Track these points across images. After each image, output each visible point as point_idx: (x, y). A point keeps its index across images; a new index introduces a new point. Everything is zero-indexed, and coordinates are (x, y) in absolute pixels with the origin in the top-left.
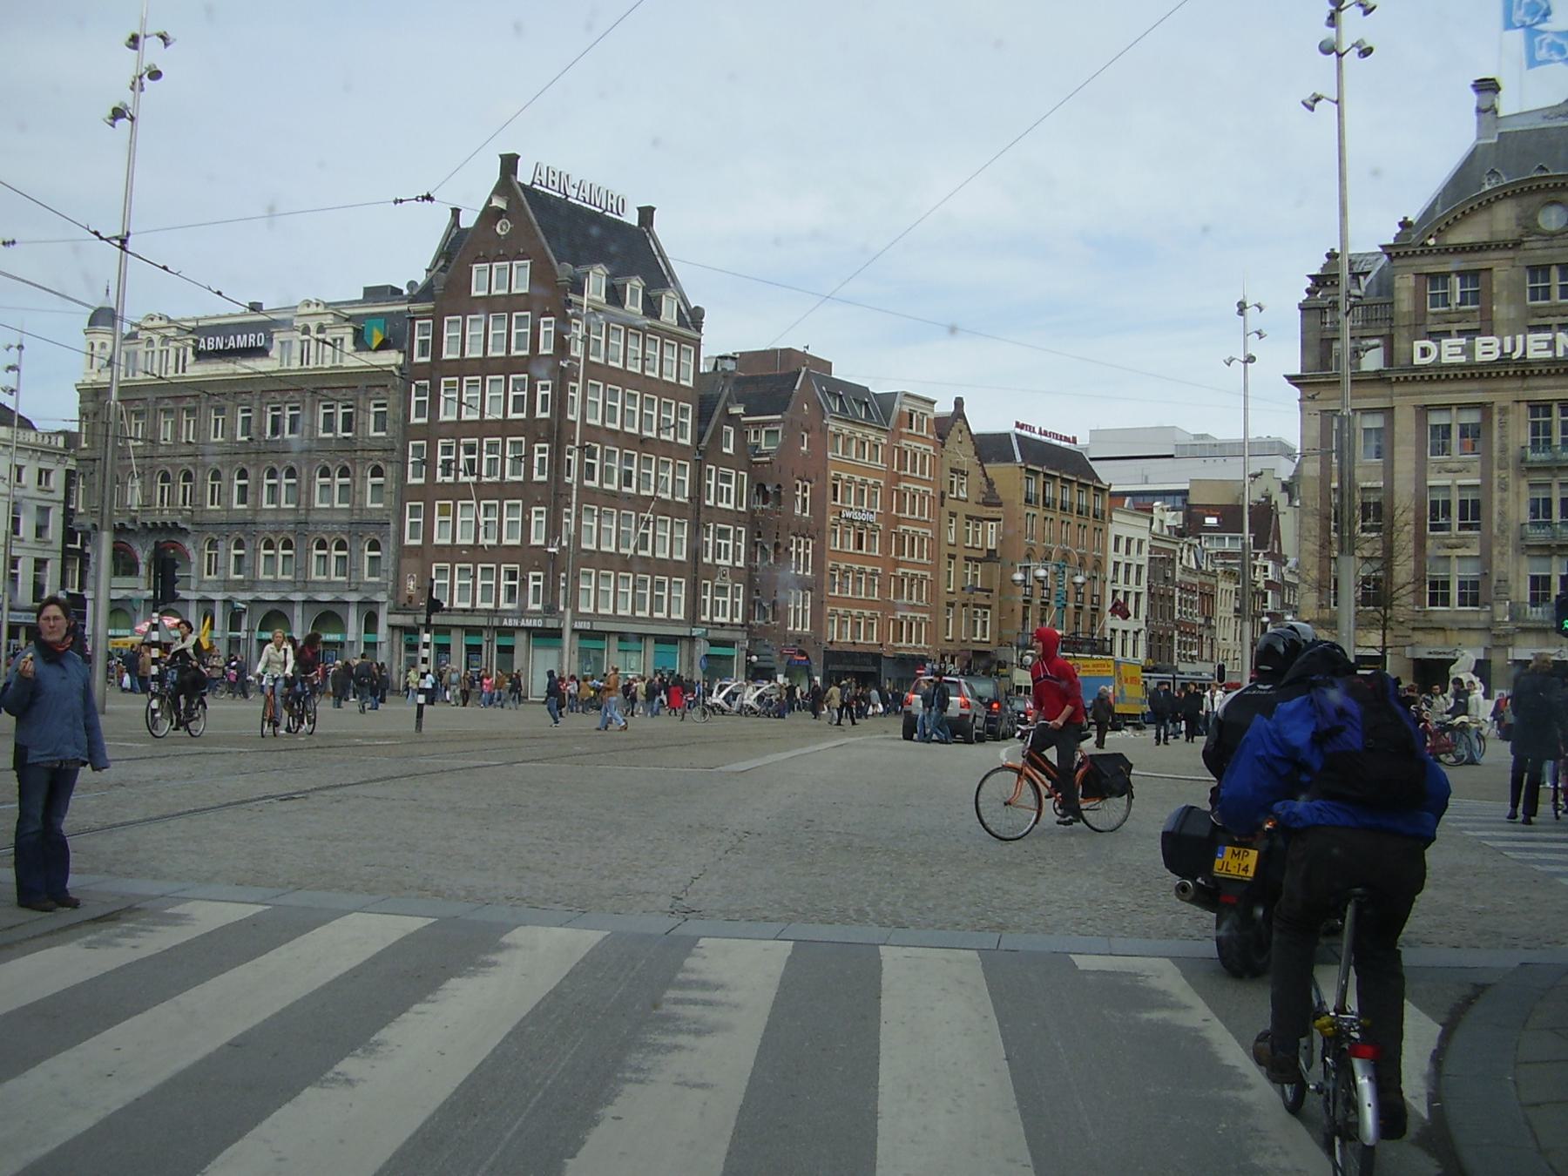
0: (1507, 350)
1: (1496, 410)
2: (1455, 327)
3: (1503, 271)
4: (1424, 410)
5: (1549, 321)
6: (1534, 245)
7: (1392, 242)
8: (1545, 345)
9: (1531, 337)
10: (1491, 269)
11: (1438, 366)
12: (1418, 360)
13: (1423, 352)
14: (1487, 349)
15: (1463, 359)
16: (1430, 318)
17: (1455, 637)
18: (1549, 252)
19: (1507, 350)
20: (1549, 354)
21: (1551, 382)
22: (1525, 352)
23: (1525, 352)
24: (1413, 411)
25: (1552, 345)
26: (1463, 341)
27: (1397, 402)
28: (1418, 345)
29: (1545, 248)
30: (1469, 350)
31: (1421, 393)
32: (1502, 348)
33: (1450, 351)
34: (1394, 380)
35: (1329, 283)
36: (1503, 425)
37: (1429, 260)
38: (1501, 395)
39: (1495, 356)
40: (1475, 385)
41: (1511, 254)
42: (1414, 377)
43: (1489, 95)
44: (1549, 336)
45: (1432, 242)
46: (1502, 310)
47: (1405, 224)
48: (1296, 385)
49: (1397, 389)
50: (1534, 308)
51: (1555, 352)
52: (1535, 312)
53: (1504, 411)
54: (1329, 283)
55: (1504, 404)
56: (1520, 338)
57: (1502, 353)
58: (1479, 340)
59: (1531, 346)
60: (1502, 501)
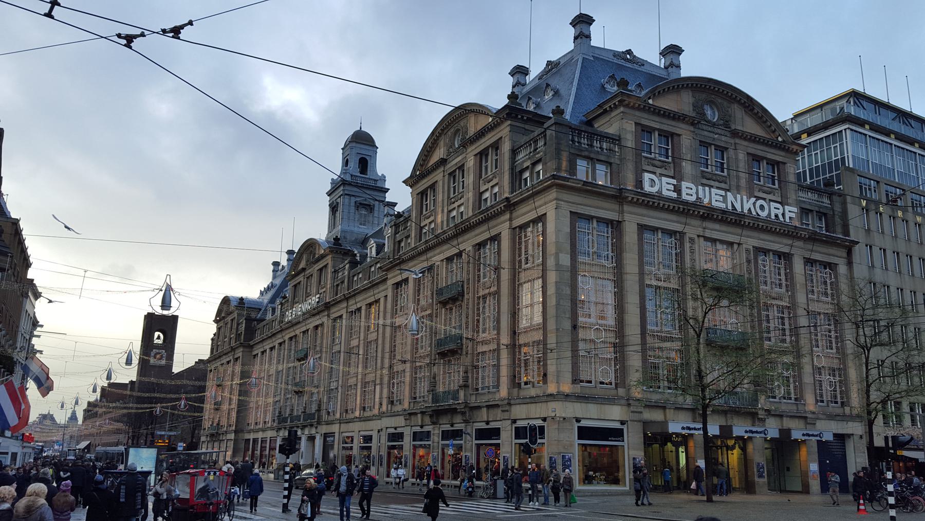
2: (659, 171)
3: (687, 139)
4: (642, 228)
5: (712, 183)
6: (704, 127)
10: (679, 135)
11: (659, 196)
12: (647, 188)
14: (690, 192)
15: (674, 195)
16: (643, 159)
17: (670, 413)
18: (711, 135)
20: (723, 206)
21: (717, 226)
24: (636, 226)
25: (725, 198)
26: (674, 182)
27: (627, 217)
29: (709, 131)
30: (677, 189)
31: (642, 215)
32: (697, 193)
34: (630, 199)
35: (520, 117)
36: (692, 251)
37: (646, 116)
38: (693, 229)
39: (693, 199)
40: (673, 217)
41: (692, 129)
42: (643, 200)
43: (583, 27)
44: (723, 193)
45: (650, 101)
46: (687, 167)
49: (626, 208)
50: (703, 171)
52: (704, 175)
53: (692, 240)
54: (520, 117)
55: (692, 236)
57: (698, 198)
59: (714, 198)
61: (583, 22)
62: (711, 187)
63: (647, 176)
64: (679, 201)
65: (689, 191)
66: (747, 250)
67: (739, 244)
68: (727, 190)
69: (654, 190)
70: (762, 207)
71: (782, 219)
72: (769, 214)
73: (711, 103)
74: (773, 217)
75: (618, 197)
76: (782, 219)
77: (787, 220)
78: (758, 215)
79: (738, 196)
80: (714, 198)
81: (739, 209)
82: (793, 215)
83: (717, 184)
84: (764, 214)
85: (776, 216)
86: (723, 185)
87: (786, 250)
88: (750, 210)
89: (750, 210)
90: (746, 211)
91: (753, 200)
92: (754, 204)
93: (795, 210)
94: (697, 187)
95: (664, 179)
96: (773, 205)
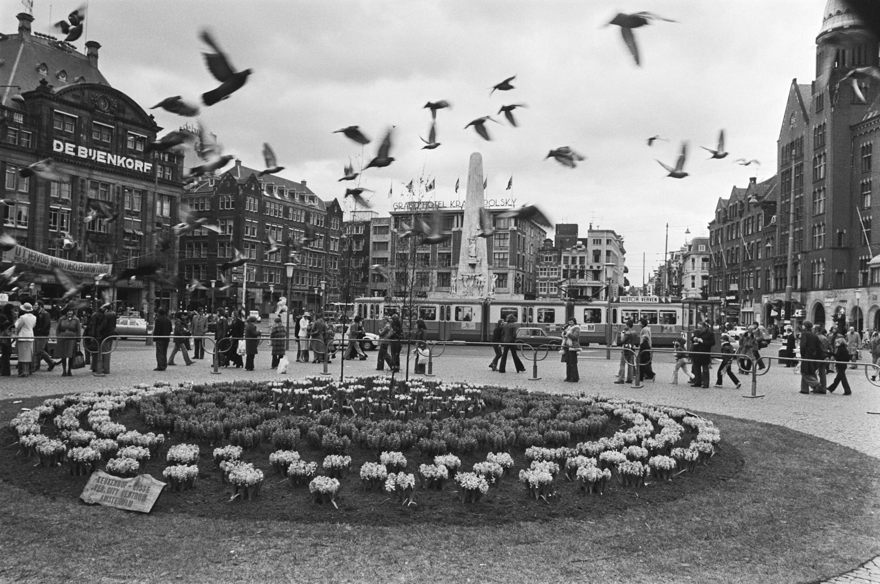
2: (64, 138)
8: (103, 157)
9: (99, 152)
12: (55, 149)
13: (58, 147)
15: (73, 154)
19: (90, 154)
20: (104, 161)
22: (96, 158)
23: (96, 158)
26: (74, 146)
28: (56, 142)
30: (76, 150)
32: (88, 153)
33: (69, 148)
38: (83, 174)
39: (85, 156)
44: (105, 154)
51: (107, 160)
53: (83, 181)
56: (95, 151)
58: (80, 148)
59: (99, 156)
61: (25, 19)
62: (98, 149)
63: (56, 142)
64: (76, 158)
65: (83, 152)
66: (118, 188)
67: (114, 184)
68: (108, 152)
69: (61, 150)
70: (130, 163)
71: (141, 170)
72: (134, 167)
73: (104, 98)
74: (136, 169)
76: (141, 170)
77: (145, 171)
78: (126, 168)
79: (115, 156)
80: (100, 156)
81: (114, 162)
82: (149, 168)
83: (102, 148)
84: (131, 167)
85: (138, 168)
86: (107, 149)
87: (143, 187)
88: (121, 164)
89: (121, 164)
90: (118, 165)
91: (124, 158)
92: (125, 161)
93: (151, 165)
94: (88, 148)
95: (67, 145)
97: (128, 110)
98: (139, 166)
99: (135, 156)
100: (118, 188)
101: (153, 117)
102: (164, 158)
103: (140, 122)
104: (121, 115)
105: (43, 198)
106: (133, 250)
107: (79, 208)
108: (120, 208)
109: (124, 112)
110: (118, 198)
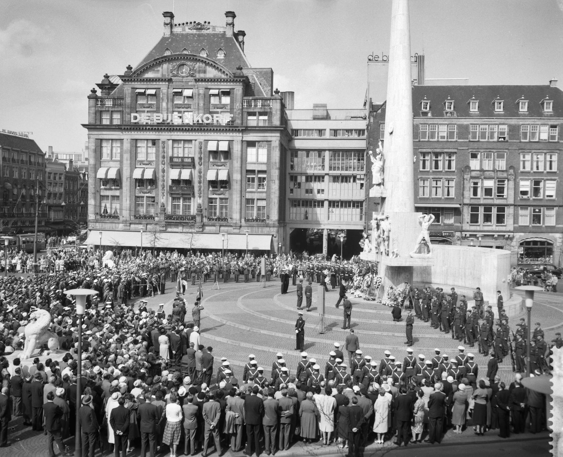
0: (165, 119)
1: (160, 142)
2: (146, 110)
7: (123, 74)
12: (133, 121)
19: (165, 119)
28: (133, 115)
38: (163, 136)
41: (167, 83)
47: (129, 68)
48: (87, 128)
50: (176, 104)
56: (170, 115)
57: (163, 120)
60: (163, 176)
65: (158, 118)
66: (201, 143)
67: (196, 140)
70: (208, 119)
75: (119, 128)
86: (189, 110)
88: (198, 121)
89: (198, 121)
91: (201, 115)
92: (202, 117)
96: (215, 115)
97: (209, 69)
98: (217, 119)
99: (219, 110)
100: (201, 143)
101: (241, 69)
102: (256, 106)
103: (223, 76)
104: (202, 76)
105: (129, 162)
106: (221, 199)
107: (161, 166)
108: (202, 161)
109: (205, 72)
110: (200, 153)
